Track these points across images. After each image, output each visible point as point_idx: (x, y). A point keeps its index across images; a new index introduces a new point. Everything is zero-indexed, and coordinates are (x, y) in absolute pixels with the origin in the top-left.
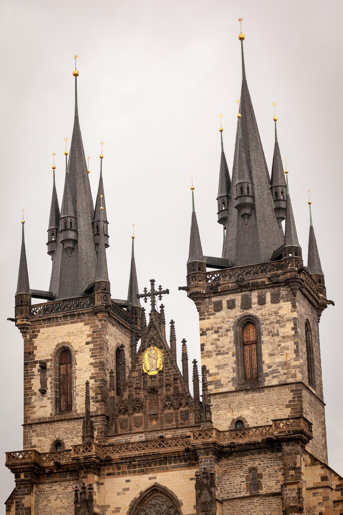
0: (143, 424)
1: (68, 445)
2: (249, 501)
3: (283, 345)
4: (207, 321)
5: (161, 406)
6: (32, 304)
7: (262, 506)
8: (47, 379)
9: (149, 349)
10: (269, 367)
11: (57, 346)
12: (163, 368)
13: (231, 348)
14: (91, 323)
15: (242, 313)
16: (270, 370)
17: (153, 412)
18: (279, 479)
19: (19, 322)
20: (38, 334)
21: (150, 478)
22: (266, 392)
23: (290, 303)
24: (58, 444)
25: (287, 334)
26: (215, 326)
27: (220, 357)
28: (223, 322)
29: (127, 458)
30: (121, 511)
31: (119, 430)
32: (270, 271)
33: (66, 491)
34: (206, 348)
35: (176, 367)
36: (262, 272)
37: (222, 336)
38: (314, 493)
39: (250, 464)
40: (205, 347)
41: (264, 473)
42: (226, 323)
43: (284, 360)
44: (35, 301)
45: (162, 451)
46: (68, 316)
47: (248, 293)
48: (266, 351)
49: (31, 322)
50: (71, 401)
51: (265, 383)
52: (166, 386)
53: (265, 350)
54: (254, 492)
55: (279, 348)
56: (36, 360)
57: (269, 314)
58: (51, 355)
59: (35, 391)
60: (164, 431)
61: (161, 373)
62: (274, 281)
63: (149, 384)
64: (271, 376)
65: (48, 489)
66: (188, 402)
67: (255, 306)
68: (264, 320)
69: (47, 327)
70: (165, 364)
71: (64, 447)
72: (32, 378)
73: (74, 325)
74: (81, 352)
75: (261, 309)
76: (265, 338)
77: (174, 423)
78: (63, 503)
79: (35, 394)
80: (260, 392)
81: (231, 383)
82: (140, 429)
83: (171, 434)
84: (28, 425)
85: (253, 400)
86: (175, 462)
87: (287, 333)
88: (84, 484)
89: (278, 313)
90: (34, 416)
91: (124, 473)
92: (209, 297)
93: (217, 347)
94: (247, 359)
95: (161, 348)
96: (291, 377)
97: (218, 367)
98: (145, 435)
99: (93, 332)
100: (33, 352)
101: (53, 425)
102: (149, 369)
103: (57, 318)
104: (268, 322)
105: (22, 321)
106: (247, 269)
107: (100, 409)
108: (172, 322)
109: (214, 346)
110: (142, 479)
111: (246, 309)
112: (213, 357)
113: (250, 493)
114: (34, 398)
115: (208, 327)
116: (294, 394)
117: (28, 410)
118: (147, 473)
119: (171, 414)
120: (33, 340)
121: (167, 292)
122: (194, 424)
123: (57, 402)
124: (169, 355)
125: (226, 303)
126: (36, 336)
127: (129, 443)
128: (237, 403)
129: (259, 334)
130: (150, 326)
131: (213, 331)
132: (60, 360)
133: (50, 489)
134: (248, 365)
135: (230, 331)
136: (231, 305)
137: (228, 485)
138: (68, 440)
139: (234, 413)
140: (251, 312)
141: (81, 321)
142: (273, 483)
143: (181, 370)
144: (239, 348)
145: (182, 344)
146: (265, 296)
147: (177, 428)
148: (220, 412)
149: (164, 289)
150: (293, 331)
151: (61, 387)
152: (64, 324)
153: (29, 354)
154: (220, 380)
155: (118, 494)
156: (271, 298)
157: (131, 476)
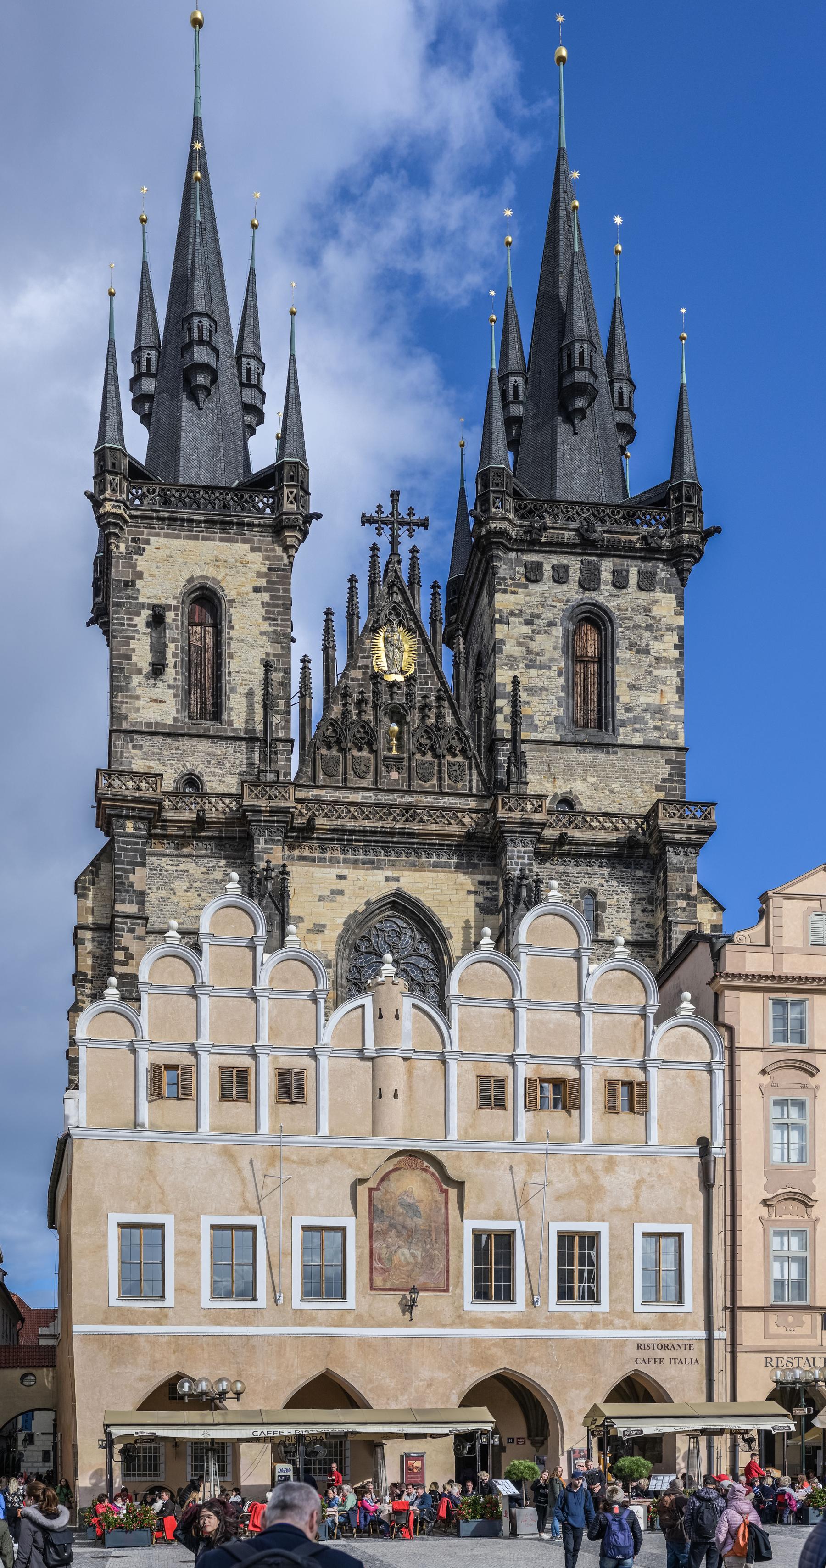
10: (628, 710)
11: (190, 580)
12: (415, 672)
13: (556, 660)
14: (266, 550)
15: (581, 596)
16: (629, 715)
20: (146, 547)
21: (387, 879)
22: (619, 755)
23: (673, 596)
24: (192, 781)
26: (528, 611)
27: (533, 673)
28: (543, 606)
29: (344, 831)
30: (327, 932)
33: (211, 876)
35: (440, 676)
37: (539, 632)
42: (550, 610)
45: (419, 828)
46: (215, 522)
47: (595, 558)
48: (624, 679)
49: (131, 517)
51: (619, 738)
53: (623, 676)
55: (649, 678)
56: (141, 600)
57: (632, 609)
58: (174, 598)
59: (139, 666)
65: (169, 867)
67: (608, 587)
68: (622, 619)
69: (166, 536)
70: (419, 665)
72: (133, 638)
73: (229, 545)
74: (243, 604)
75: (619, 596)
76: (622, 653)
79: (139, 671)
80: (608, 753)
81: (553, 727)
82: (367, 782)
84: (119, 730)
85: (593, 765)
87: (666, 651)
88: (268, 862)
89: (650, 610)
90: (133, 716)
91: (334, 861)
92: (517, 551)
93: (529, 651)
98: (376, 795)
99: (269, 569)
100: (134, 583)
101: (180, 743)
102: (386, 669)
103: (191, 521)
104: (631, 624)
106: (598, 510)
109: (524, 649)
110: (370, 878)
111: (589, 590)
114: (136, 680)
115: (512, 608)
117: (123, 702)
118: (382, 869)
119: (431, 763)
120: (135, 557)
125: (550, 569)
126: (140, 551)
132: (192, 613)
133: (175, 868)
136: (560, 576)
138: (212, 778)
139: (558, 784)
141: (244, 541)
146: (628, 571)
150: (677, 652)
155: (321, 898)
157: (349, 868)
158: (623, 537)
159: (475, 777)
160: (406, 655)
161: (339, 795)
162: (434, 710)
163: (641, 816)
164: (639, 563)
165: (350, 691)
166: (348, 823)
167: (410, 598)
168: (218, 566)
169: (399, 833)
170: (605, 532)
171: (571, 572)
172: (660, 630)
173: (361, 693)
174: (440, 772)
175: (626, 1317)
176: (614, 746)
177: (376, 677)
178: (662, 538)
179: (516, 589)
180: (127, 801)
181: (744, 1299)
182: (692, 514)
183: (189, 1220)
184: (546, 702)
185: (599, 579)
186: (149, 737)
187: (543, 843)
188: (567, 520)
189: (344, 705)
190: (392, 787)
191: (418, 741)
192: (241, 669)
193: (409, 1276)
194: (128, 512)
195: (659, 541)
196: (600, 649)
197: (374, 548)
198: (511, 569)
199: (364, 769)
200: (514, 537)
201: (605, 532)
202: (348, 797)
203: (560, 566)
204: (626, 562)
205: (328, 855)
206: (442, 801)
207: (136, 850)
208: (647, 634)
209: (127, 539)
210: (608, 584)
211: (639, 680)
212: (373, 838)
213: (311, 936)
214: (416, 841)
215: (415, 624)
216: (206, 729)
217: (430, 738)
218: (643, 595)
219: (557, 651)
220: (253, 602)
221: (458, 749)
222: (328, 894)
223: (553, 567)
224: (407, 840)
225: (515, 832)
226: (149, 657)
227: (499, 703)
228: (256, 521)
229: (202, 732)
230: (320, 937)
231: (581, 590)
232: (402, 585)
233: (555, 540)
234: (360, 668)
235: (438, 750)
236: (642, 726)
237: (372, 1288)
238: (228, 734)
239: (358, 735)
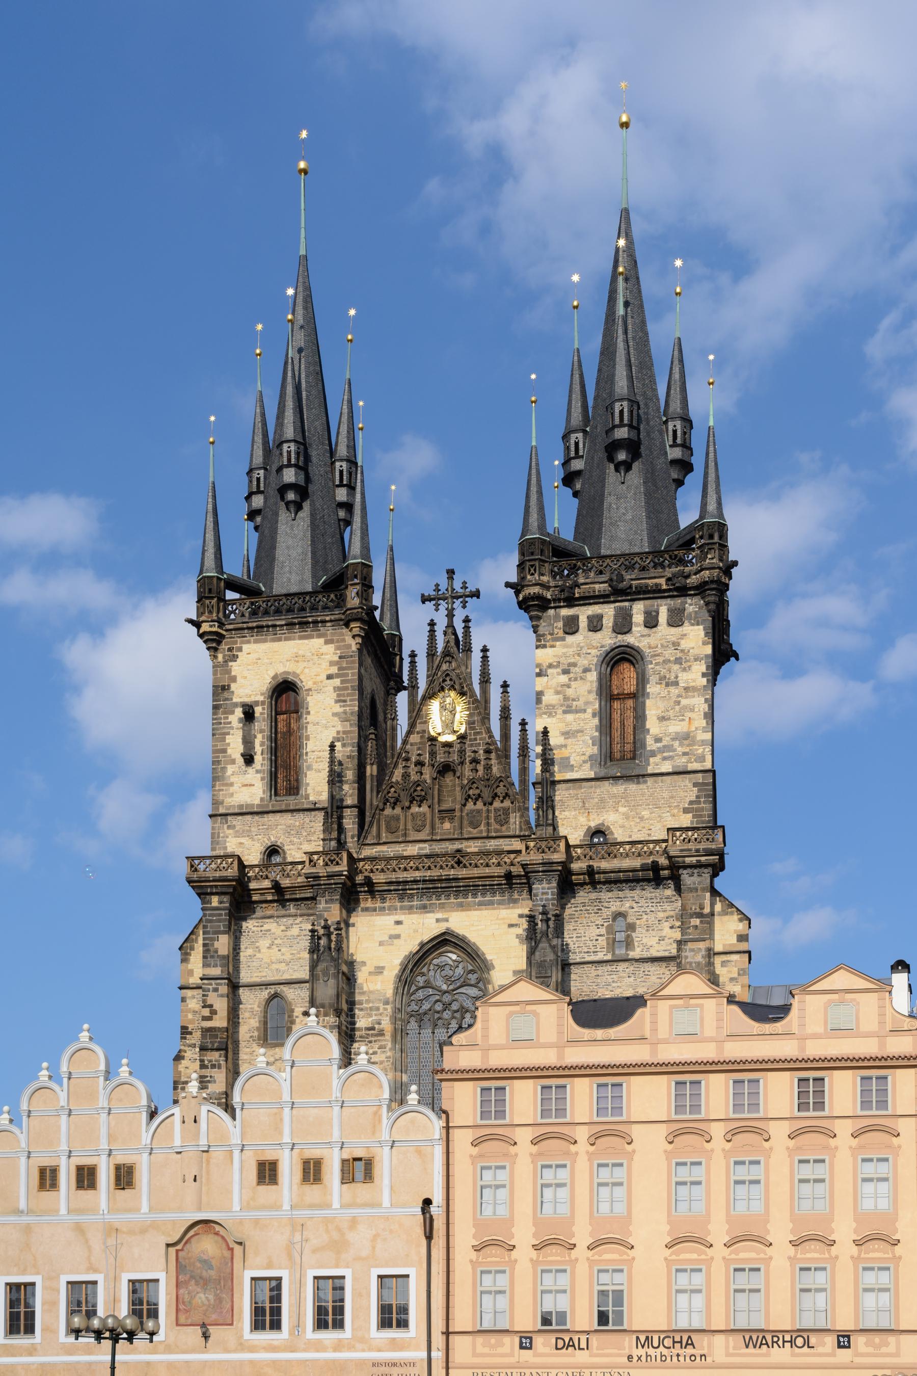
0: (427, 826)
1: (294, 854)
2: (609, 967)
3: (684, 702)
4: (549, 651)
6: (227, 598)
7: (632, 979)
8: (255, 737)
9: (441, 695)
10: (658, 740)
11: (274, 678)
14: (338, 641)
15: (615, 640)
16: (659, 745)
18: (664, 934)
19: (205, 627)
20: (239, 654)
21: (438, 920)
23: (701, 627)
27: (570, 717)
28: (579, 655)
29: (398, 883)
30: (385, 973)
32: (670, 566)
33: (289, 933)
34: (545, 699)
35: (489, 731)
36: (655, 567)
37: (576, 679)
38: (723, 962)
39: (615, 906)
41: (638, 922)
43: (685, 730)
44: (230, 595)
45: (462, 873)
46: (295, 624)
47: (627, 604)
48: (654, 712)
50: (297, 780)
53: (653, 709)
54: (621, 952)
55: (677, 708)
56: (235, 700)
57: (662, 646)
58: (262, 694)
59: (233, 757)
60: (464, 841)
63: (441, 758)
64: (659, 757)
65: (255, 929)
66: (510, 792)
67: (639, 629)
69: (256, 642)
70: (470, 724)
71: (285, 858)
72: (228, 734)
73: (306, 641)
74: (319, 691)
75: (649, 635)
76: (652, 688)
77: (482, 827)
78: (283, 954)
79: (233, 762)
80: (638, 783)
81: (588, 765)
83: (476, 847)
85: (625, 796)
87: (694, 681)
88: (326, 920)
89: (679, 644)
91: (393, 909)
92: (555, 608)
93: (566, 698)
94: (616, 724)
95: (462, 694)
96: (696, 761)
97: (566, 734)
99: (340, 657)
100: (229, 686)
101: (266, 819)
102: (440, 731)
103: (274, 626)
104: (661, 659)
106: (628, 560)
107: (351, 796)
108: (485, 650)
109: (561, 696)
112: (558, 716)
113: (613, 954)
114: (230, 769)
115: (551, 661)
116: (699, 791)
117: (220, 790)
118: (433, 912)
119: (479, 811)
120: (230, 664)
122: (517, 833)
123: (273, 777)
124: (480, 708)
125: (585, 620)
126: (234, 658)
128: (596, 800)
129: (642, 680)
131: (559, 670)
133: (259, 929)
134: (617, 735)
136: (595, 625)
137: (574, 939)
138: (292, 847)
139: (592, 817)
140: (630, 639)
141: (319, 636)
142: (653, 941)
143: (497, 735)
144: (603, 703)
145: (501, 690)
147: (488, 837)
148: (567, 813)
149: (471, 588)
150: (705, 680)
151: (279, 754)
152: (287, 639)
153: (221, 690)
154: (568, 758)
155: (381, 944)
156: (669, 616)
158: (650, 582)
162: (482, 763)
164: (669, 601)
165: (410, 755)
166: (402, 876)
168: (298, 662)
169: (446, 880)
170: (632, 580)
171: (604, 621)
172: (688, 661)
173: (419, 755)
175: (361, 1340)
176: (643, 776)
177: (433, 739)
180: (210, 881)
181: (455, 1326)
183: (52, 1278)
186: (240, 818)
190: (444, 837)
192: (315, 748)
193: (204, 1314)
195: (683, 580)
197: (432, 624)
198: (550, 625)
200: (549, 597)
201: (632, 580)
203: (593, 616)
204: (656, 602)
205: (387, 905)
207: (220, 921)
208: (676, 667)
209: (224, 649)
211: (668, 711)
213: (373, 978)
216: (287, 805)
217: (477, 788)
218: (673, 630)
220: (326, 689)
222: (386, 938)
225: (539, 872)
226: (241, 748)
228: (328, 618)
229: (283, 808)
230: (380, 978)
231: (615, 634)
233: (587, 594)
234: (418, 733)
237: (177, 1325)
238: (305, 806)
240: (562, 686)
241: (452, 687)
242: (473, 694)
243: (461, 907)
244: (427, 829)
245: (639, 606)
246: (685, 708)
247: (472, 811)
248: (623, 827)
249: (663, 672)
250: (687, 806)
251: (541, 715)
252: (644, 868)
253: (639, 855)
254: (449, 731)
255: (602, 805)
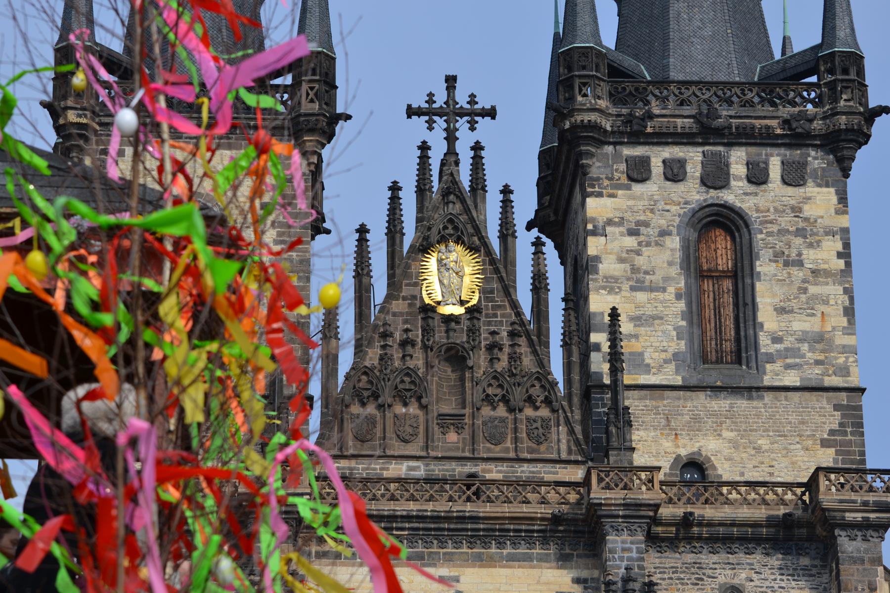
4: (605, 201)
5: (474, 394)
9: (443, 247)
10: (776, 340)
13: (673, 279)
16: (778, 346)
17: (446, 409)
23: (832, 190)
25: (826, 266)
27: (641, 296)
28: (652, 211)
31: (351, 443)
37: (648, 244)
40: (600, 266)
42: (661, 215)
43: (817, 328)
47: (721, 148)
48: (768, 300)
51: (765, 378)
52: (490, 348)
53: (766, 298)
55: (803, 297)
57: (776, 209)
61: (476, 315)
62: (800, 130)
63: (439, 336)
67: (740, 184)
68: (762, 223)
75: (756, 194)
76: (764, 266)
80: (750, 398)
81: (672, 367)
82: (413, 449)
85: (730, 415)
86: (514, 545)
87: (826, 262)
89: (800, 210)
92: (615, 144)
97: (637, 320)
98: (427, 465)
102: (440, 298)
104: (775, 228)
105: (79, 116)
108: (506, 191)
109: (627, 266)
111: (715, 188)
112: (624, 293)
115: (610, 215)
118: (434, 565)
119: (503, 420)
121: (491, 113)
122: (564, 456)
125: (660, 164)
127: (380, 480)
130: (445, 193)
131: (623, 229)
135: (669, 234)
136: (675, 172)
139: (681, 442)
140: (728, 197)
146: (766, 163)
154: (641, 354)
156: (783, 170)
159: (564, 437)
160: (467, 280)
161: (376, 467)
162: (507, 350)
163: (800, 485)
164: (782, 151)
165: (391, 329)
167: (472, 207)
171: (689, 168)
172: (816, 234)
173: (407, 331)
174: (516, 430)
177: (428, 311)
178: (811, 121)
179: (615, 191)
182: (850, 90)
184: (660, 334)
185: (728, 174)
187: (660, 524)
188: (682, 104)
189: (384, 347)
191: (484, 391)
194: (97, 120)
196: (735, 265)
197: (424, 147)
198: (607, 166)
199: (409, 430)
202: (388, 469)
204: (764, 151)
206: (519, 470)
208: (799, 241)
210: (740, 179)
211: (790, 300)
212: (421, 525)
214: (482, 526)
215: (479, 239)
217: (500, 386)
218: (790, 190)
219: (674, 268)
221: (539, 399)
223: (664, 162)
224: (469, 526)
227: (595, 338)
231: (704, 189)
232: (460, 191)
234: (404, 298)
235: (512, 403)
236: (797, 360)
239: (401, 386)
240: (628, 251)
241: (459, 241)
242: (489, 252)
243: (480, 561)
244: (421, 440)
245: (739, 153)
246: (815, 297)
247: (492, 419)
248: (729, 459)
249: (779, 246)
250: (826, 436)
251: (597, 290)
252: (771, 522)
253: (765, 502)
254: (454, 301)
255: (696, 425)
